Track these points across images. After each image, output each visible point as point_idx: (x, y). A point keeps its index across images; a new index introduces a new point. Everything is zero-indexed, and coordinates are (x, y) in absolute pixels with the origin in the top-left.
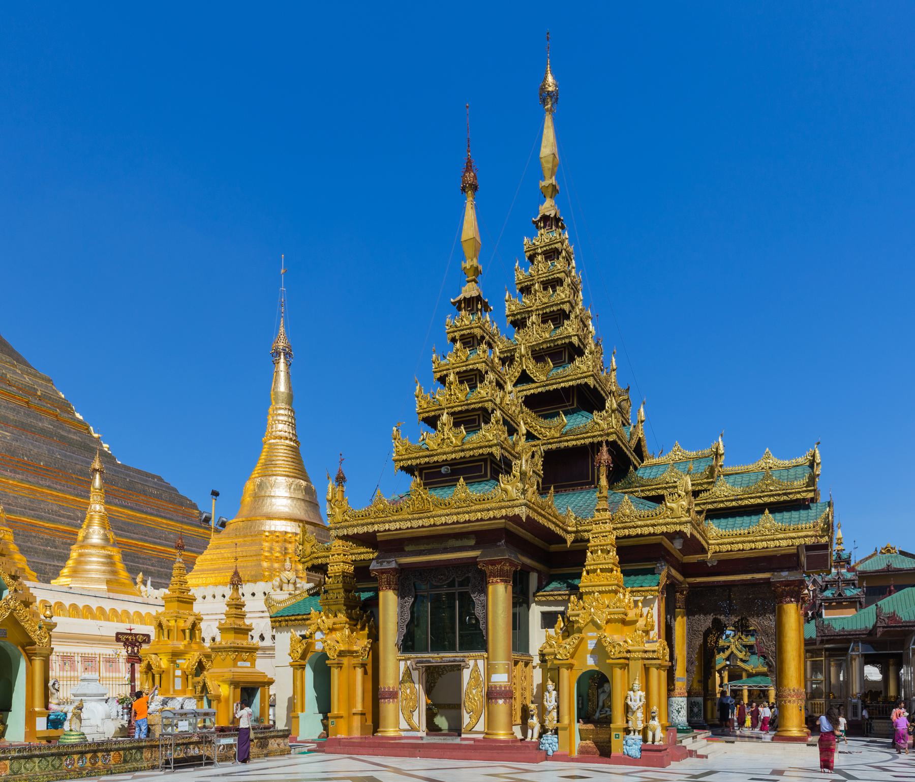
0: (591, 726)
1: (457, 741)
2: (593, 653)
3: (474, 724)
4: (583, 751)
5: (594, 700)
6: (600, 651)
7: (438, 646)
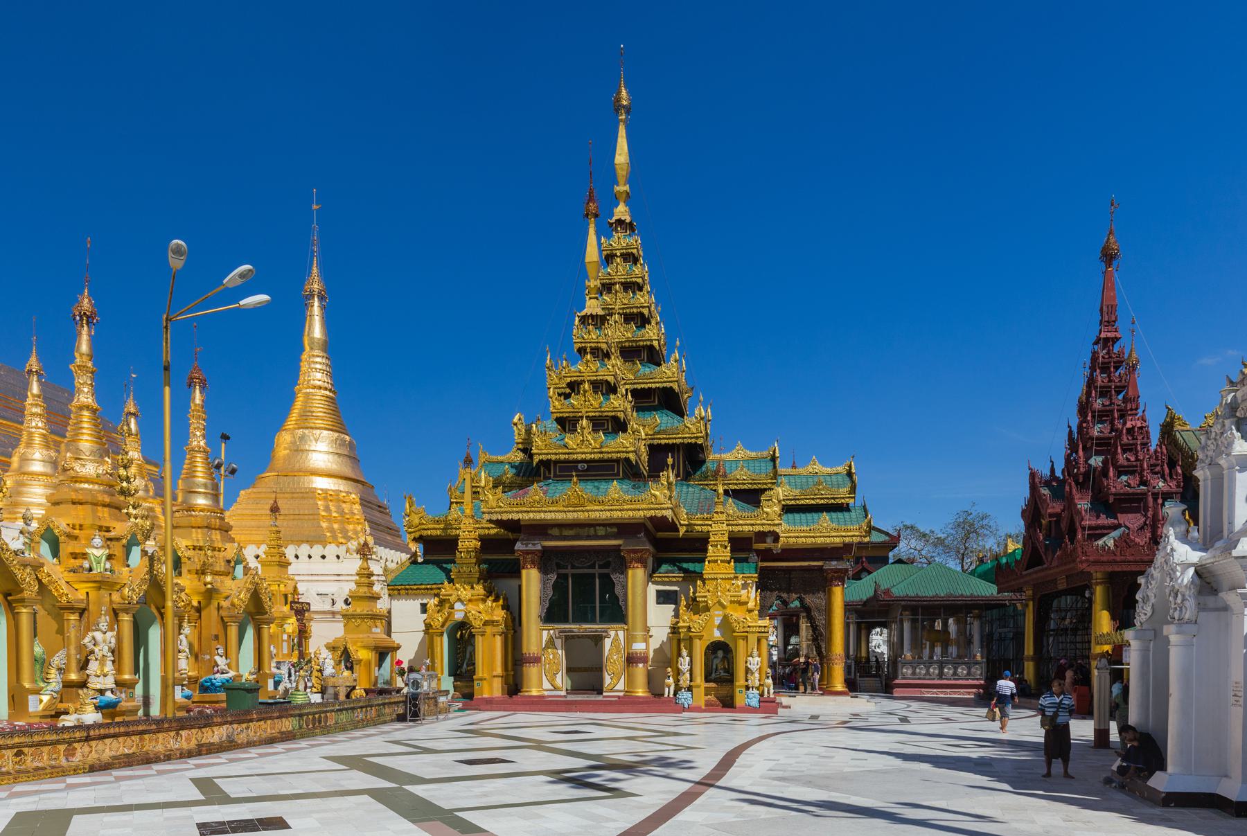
0: (713, 685)
1: (600, 698)
2: (719, 627)
3: (614, 683)
4: (708, 704)
5: (721, 664)
6: (726, 624)
7: (582, 618)
